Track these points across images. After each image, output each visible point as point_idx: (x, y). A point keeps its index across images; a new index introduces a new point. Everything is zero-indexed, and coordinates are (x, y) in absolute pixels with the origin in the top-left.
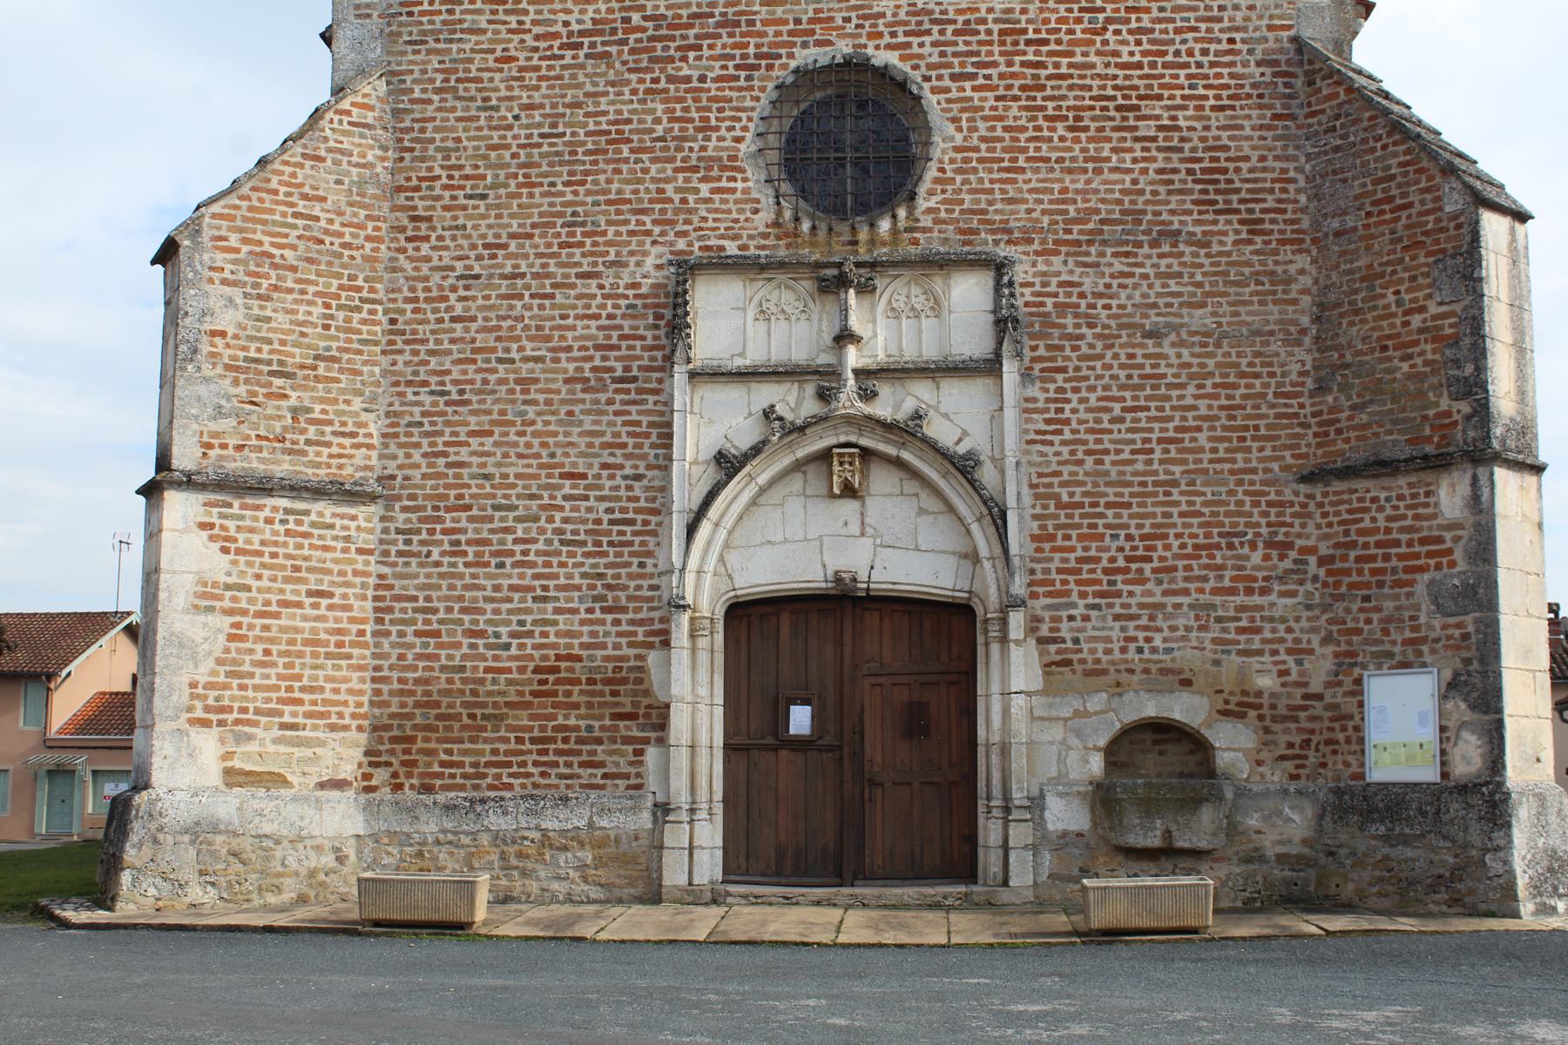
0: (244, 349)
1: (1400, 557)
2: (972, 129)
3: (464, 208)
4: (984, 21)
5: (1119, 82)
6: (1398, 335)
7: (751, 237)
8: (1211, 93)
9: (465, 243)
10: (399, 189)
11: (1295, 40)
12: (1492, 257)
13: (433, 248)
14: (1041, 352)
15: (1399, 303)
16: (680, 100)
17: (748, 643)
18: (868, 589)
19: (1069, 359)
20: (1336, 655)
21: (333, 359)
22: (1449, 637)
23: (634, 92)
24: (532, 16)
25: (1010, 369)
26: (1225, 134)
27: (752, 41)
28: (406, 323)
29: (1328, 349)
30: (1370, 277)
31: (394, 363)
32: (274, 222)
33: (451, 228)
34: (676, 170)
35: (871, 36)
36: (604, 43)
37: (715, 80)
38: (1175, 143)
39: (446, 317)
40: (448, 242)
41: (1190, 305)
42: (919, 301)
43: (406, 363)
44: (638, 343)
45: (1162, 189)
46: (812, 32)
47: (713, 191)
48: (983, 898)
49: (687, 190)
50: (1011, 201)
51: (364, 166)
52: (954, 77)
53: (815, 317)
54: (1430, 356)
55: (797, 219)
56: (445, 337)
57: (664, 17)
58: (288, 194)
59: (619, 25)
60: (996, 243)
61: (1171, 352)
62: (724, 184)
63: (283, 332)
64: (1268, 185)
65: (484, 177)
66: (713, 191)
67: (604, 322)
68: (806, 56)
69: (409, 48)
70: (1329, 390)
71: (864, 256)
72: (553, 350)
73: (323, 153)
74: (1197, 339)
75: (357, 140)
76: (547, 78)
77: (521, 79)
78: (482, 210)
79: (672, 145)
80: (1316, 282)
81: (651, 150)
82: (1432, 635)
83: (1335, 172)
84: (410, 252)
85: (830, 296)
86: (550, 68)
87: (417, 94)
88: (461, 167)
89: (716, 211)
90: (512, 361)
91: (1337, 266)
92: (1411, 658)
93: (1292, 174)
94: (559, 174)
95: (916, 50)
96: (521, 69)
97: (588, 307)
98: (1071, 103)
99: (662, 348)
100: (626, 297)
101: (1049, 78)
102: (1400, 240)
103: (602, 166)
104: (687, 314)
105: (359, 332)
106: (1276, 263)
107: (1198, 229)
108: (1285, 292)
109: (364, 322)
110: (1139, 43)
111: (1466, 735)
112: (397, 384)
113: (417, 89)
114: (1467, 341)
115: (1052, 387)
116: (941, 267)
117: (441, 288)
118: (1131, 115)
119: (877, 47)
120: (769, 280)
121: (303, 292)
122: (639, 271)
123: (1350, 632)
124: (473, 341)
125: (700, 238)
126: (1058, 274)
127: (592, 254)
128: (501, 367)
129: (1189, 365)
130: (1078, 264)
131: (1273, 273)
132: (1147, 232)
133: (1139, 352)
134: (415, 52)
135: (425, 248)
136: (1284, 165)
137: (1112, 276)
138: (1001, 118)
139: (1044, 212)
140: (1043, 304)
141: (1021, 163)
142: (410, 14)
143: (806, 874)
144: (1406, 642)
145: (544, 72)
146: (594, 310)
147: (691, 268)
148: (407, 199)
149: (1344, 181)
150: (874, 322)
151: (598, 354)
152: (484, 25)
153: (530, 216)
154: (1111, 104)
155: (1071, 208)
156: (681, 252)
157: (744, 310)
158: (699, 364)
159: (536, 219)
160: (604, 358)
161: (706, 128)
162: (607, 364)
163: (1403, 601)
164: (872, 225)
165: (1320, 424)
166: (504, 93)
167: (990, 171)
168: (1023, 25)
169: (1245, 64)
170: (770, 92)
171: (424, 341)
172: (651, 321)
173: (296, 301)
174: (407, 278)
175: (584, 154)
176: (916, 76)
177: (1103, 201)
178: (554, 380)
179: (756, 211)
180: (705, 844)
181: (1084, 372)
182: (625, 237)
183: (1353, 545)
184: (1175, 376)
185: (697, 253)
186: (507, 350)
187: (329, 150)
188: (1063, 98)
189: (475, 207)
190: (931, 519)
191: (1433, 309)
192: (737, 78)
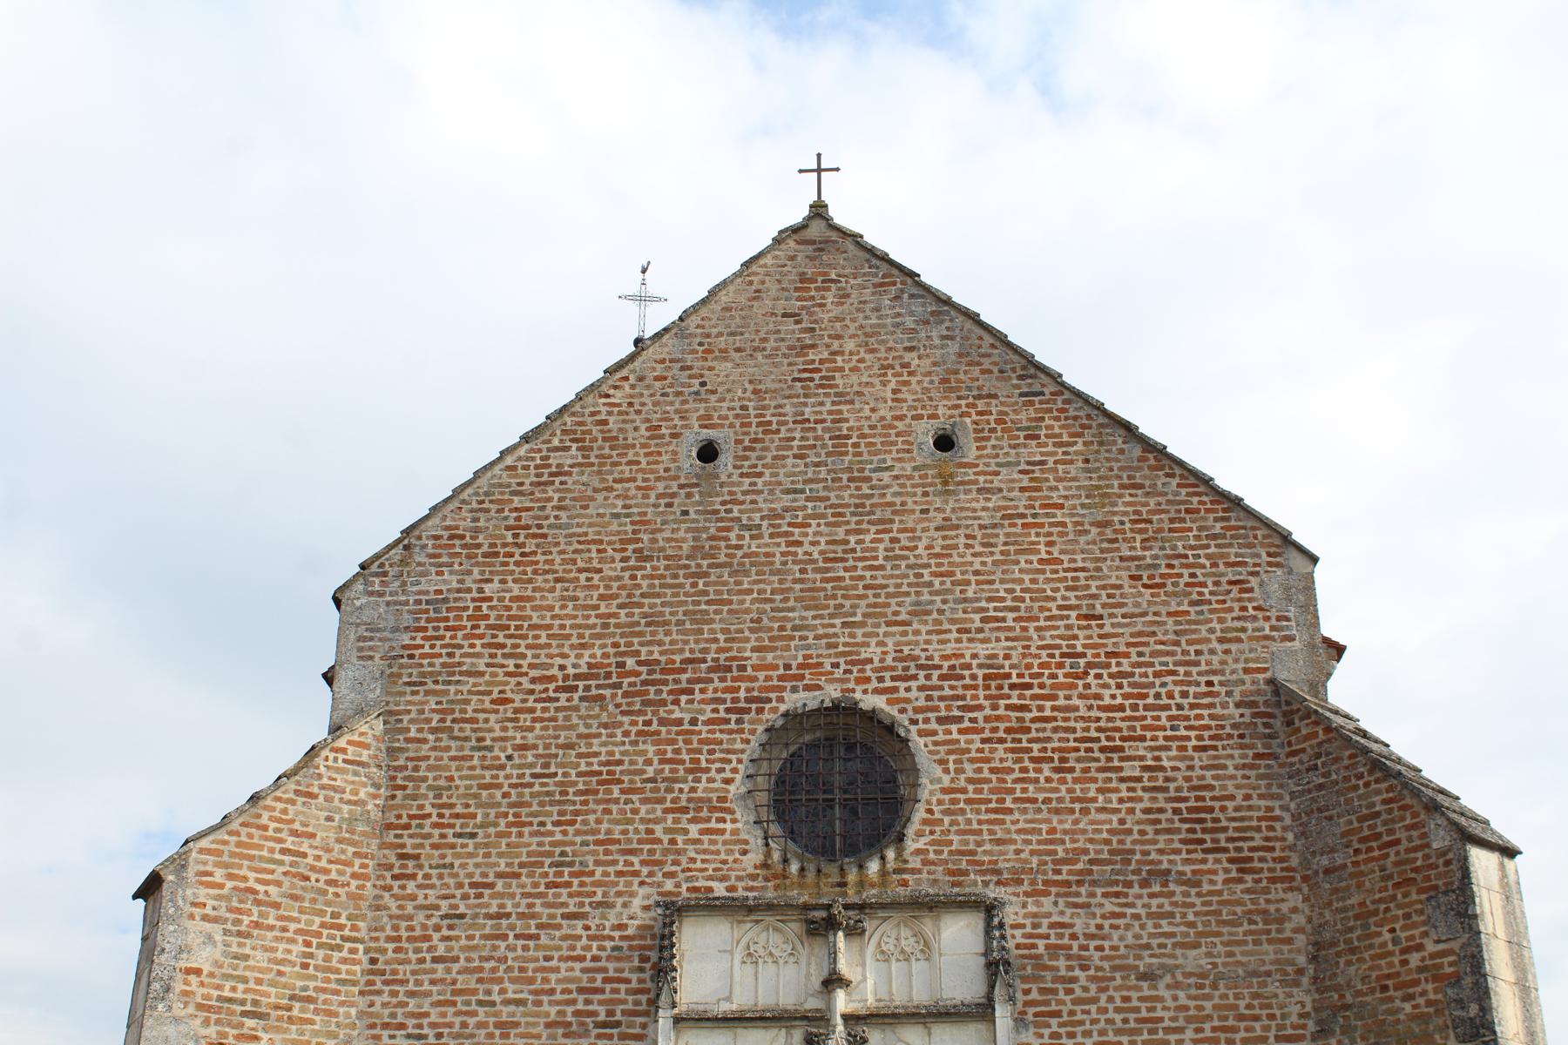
0: (219, 987)
2: (959, 771)
3: (453, 846)
4: (968, 667)
5: (1102, 724)
6: (1398, 974)
7: (739, 878)
8: (1193, 734)
9: (451, 882)
10: (389, 827)
11: (1271, 682)
12: (1484, 893)
13: (419, 887)
14: (1034, 995)
15: (1395, 942)
16: (672, 742)
19: (1063, 1003)
21: (309, 1000)
23: (626, 734)
24: (529, 660)
25: (1002, 1013)
26: (1208, 774)
27: (743, 685)
28: (387, 963)
29: (1328, 989)
30: (1364, 915)
31: (372, 1005)
32: (261, 858)
33: (438, 866)
34: (666, 811)
35: (859, 681)
36: (598, 687)
37: (706, 723)
38: (1160, 783)
39: (428, 957)
40: (434, 880)
41: (1184, 946)
42: (909, 943)
43: (384, 1005)
44: (623, 987)
45: (1149, 828)
46: (802, 677)
47: (702, 832)
49: (676, 831)
50: (999, 842)
51: (355, 803)
52: (940, 720)
53: (803, 960)
54: (1432, 996)
55: (785, 861)
56: (425, 978)
57: (658, 662)
58: (278, 830)
59: (613, 669)
60: (986, 884)
61: (1166, 994)
62: (713, 825)
63: (261, 970)
64: (1254, 823)
65: (474, 816)
66: (702, 832)
67: (588, 964)
68: (795, 700)
69: (408, 689)
70: (1332, 1033)
71: (853, 897)
72: (536, 993)
73: (315, 790)
74: (1192, 980)
75: (350, 777)
76: (542, 720)
77: (516, 720)
78: (471, 849)
79: (663, 786)
80: (1310, 920)
81: (641, 791)
83: (1320, 810)
84: (396, 890)
85: (819, 940)
86: (544, 710)
87: (412, 734)
88: (452, 806)
89: (705, 852)
90: (493, 1004)
91: (1330, 904)
93: (1278, 812)
94: (550, 814)
95: (902, 694)
96: (516, 711)
97: (573, 948)
98: (1056, 745)
99: (648, 991)
100: (612, 938)
101: (1033, 720)
102: (1390, 877)
103: (591, 806)
104: (673, 956)
105: (338, 971)
106: (1268, 901)
107: (1188, 869)
108: (1279, 931)
109: (344, 961)
110: (1119, 686)
112: (373, 1026)
113: (413, 728)
114: (1468, 981)
115: (1046, 1032)
116: (931, 909)
117: (424, 927)
118: (1115, 756)
119: (865, 692)
120: (757, 922)
121: (284, 929)
122: (626, 912)
124: (454, 982)
125: (688, 879)
126: (1049, 915)
127: (579, 894)
128: (481, 1010)
129: (1186, 1008)
130: (1068, 905)
131: (1265, 912)
132: (1137, 872)
133: (1134, 995)
134: (414, 693)
135: (411, 886)
136: (1269, 803)
137: (1103, 917)
138: (988, 760)
139: (1032, 853)
140: (1034, 946)
141: (1009, 804)
142: (411, 657)
145: (538, 714)
146: (579, 952)
147: (679, 910)
148: (397, 836)
149: (1330, 818)
150: (863, 965)
151: (581, 998)
152: (482, 668)
153: (518, 855)
154: (1095, 746)
155: (1060, 849)
156: (670, 893)
157: (731, 952)
158: (684, 1008)
159: (524, 859)
160: (587, 1002)
161: (696, 770)
162: (590, 1008)
164: (861, 867)
166: (498, 734)
167: (978, 812)
168: (1007, 670)
169: (1224, 705)
170: (760, 735)
171: (403, 982)
172: (636, 963)
173: (276, 939)
174: (391, 917)
175: (575, 794)
176: (904, 719)
177: (1091, 841)
178: (535, 1024)
179: (745, 853)
181: (1079, 1017)
182: (612, 878)
184: (1173, 1019)
185: (685, 894)
186: (489, 992)
187: (322, 787)
188: (1049, 739)
189: (464, 846)
191: (1431, 947)
192: (728, 721)
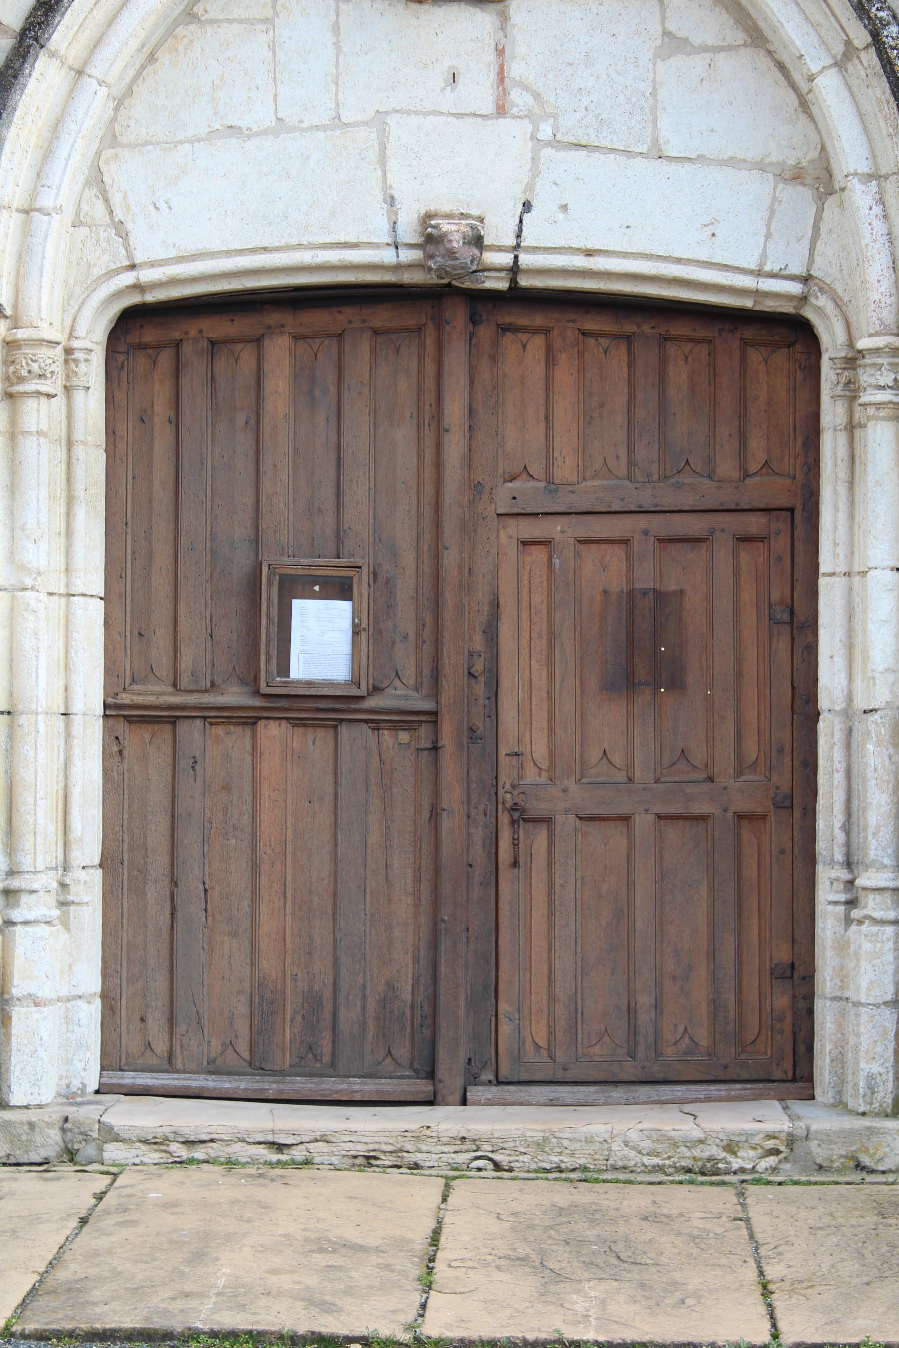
17: (176, 422)
18: (515, 269)
48: (838, 1151)
143: (333, 1068)
180: (45, 991)
190: (697, 64)
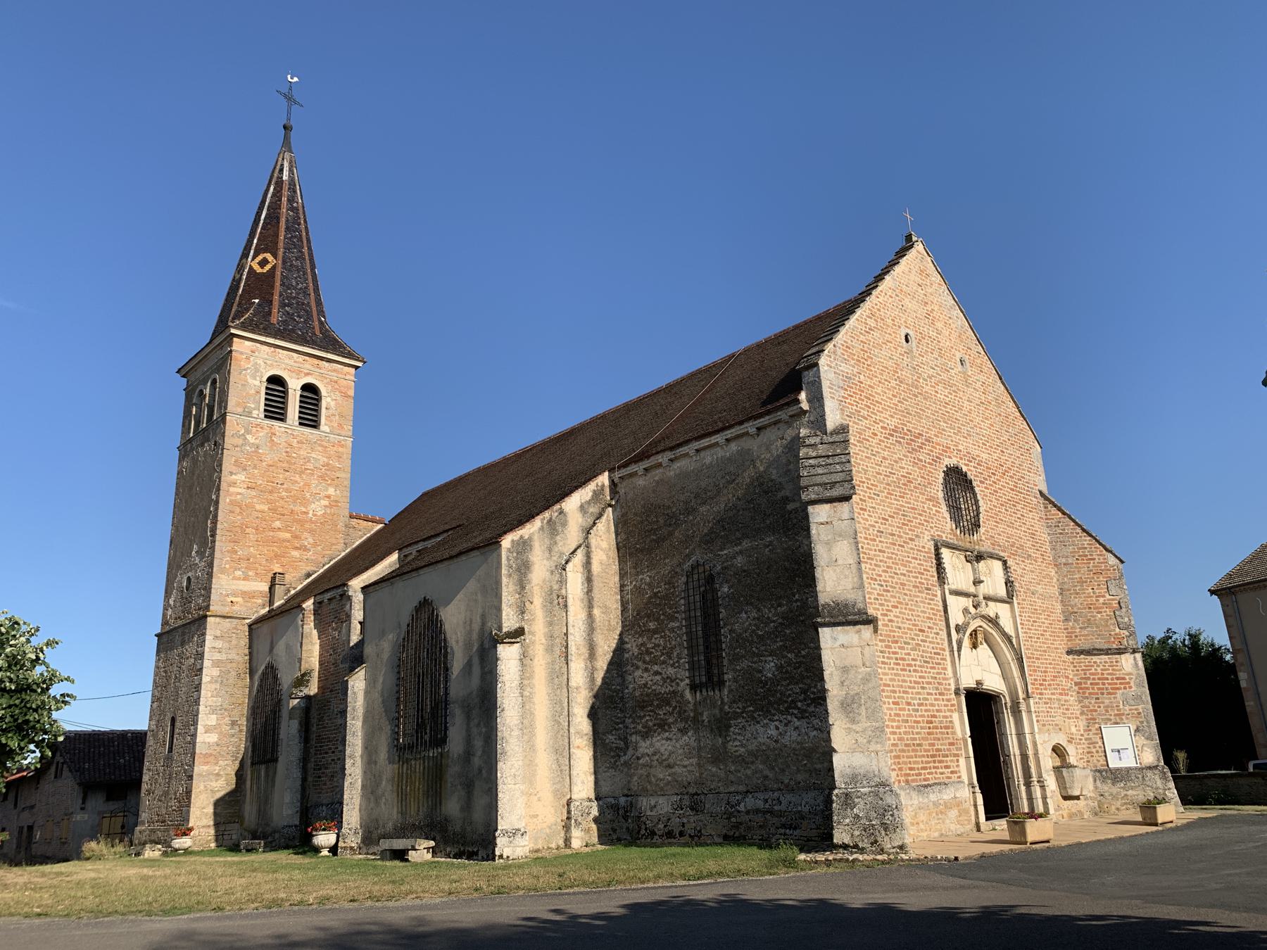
1: (1109, 684)
20: (1087, 719)
22: (1133, 714)
30: (1081, 582)
82: (1126, 713)
92: (1118, 721)
111: (1145, 748)
123: (1091, 711)
144: (1115, 715)
163: (1113, 700)
165: (1068, 633)
183: (1089, 678)
